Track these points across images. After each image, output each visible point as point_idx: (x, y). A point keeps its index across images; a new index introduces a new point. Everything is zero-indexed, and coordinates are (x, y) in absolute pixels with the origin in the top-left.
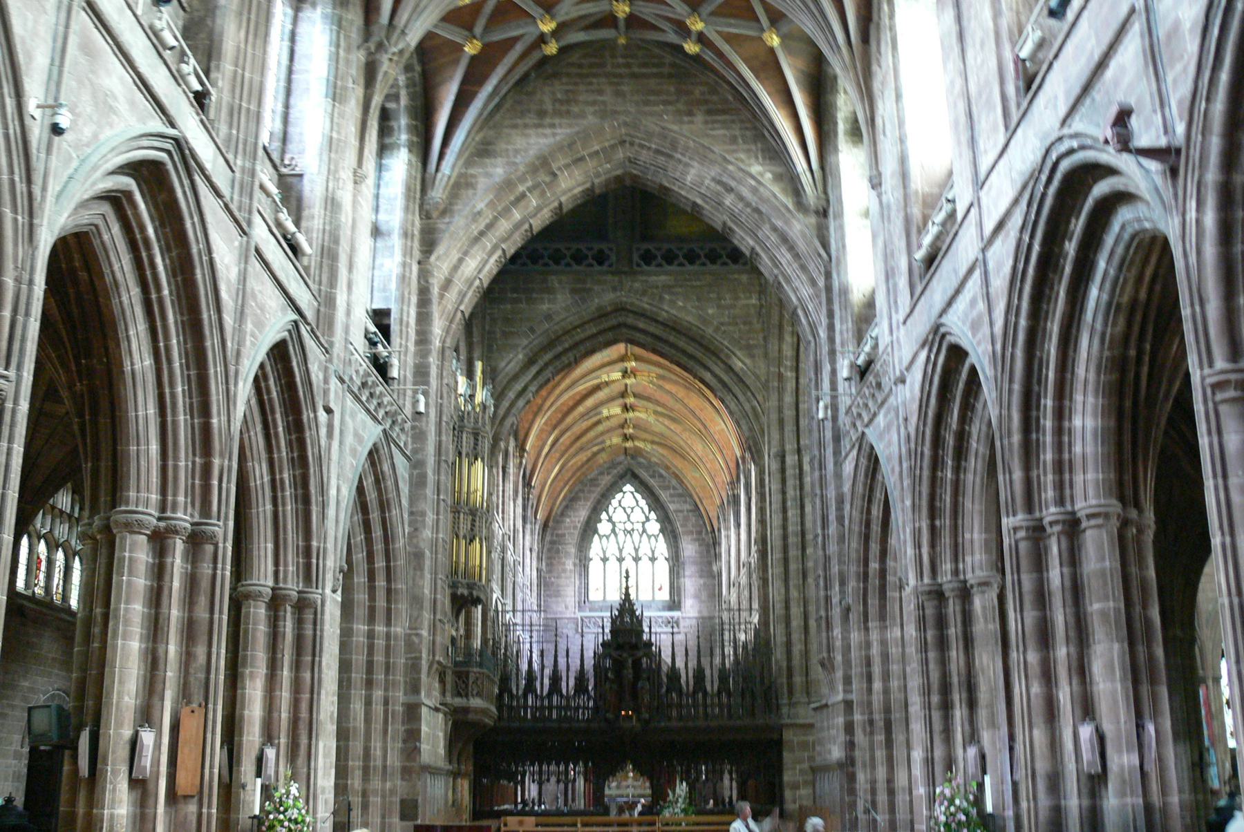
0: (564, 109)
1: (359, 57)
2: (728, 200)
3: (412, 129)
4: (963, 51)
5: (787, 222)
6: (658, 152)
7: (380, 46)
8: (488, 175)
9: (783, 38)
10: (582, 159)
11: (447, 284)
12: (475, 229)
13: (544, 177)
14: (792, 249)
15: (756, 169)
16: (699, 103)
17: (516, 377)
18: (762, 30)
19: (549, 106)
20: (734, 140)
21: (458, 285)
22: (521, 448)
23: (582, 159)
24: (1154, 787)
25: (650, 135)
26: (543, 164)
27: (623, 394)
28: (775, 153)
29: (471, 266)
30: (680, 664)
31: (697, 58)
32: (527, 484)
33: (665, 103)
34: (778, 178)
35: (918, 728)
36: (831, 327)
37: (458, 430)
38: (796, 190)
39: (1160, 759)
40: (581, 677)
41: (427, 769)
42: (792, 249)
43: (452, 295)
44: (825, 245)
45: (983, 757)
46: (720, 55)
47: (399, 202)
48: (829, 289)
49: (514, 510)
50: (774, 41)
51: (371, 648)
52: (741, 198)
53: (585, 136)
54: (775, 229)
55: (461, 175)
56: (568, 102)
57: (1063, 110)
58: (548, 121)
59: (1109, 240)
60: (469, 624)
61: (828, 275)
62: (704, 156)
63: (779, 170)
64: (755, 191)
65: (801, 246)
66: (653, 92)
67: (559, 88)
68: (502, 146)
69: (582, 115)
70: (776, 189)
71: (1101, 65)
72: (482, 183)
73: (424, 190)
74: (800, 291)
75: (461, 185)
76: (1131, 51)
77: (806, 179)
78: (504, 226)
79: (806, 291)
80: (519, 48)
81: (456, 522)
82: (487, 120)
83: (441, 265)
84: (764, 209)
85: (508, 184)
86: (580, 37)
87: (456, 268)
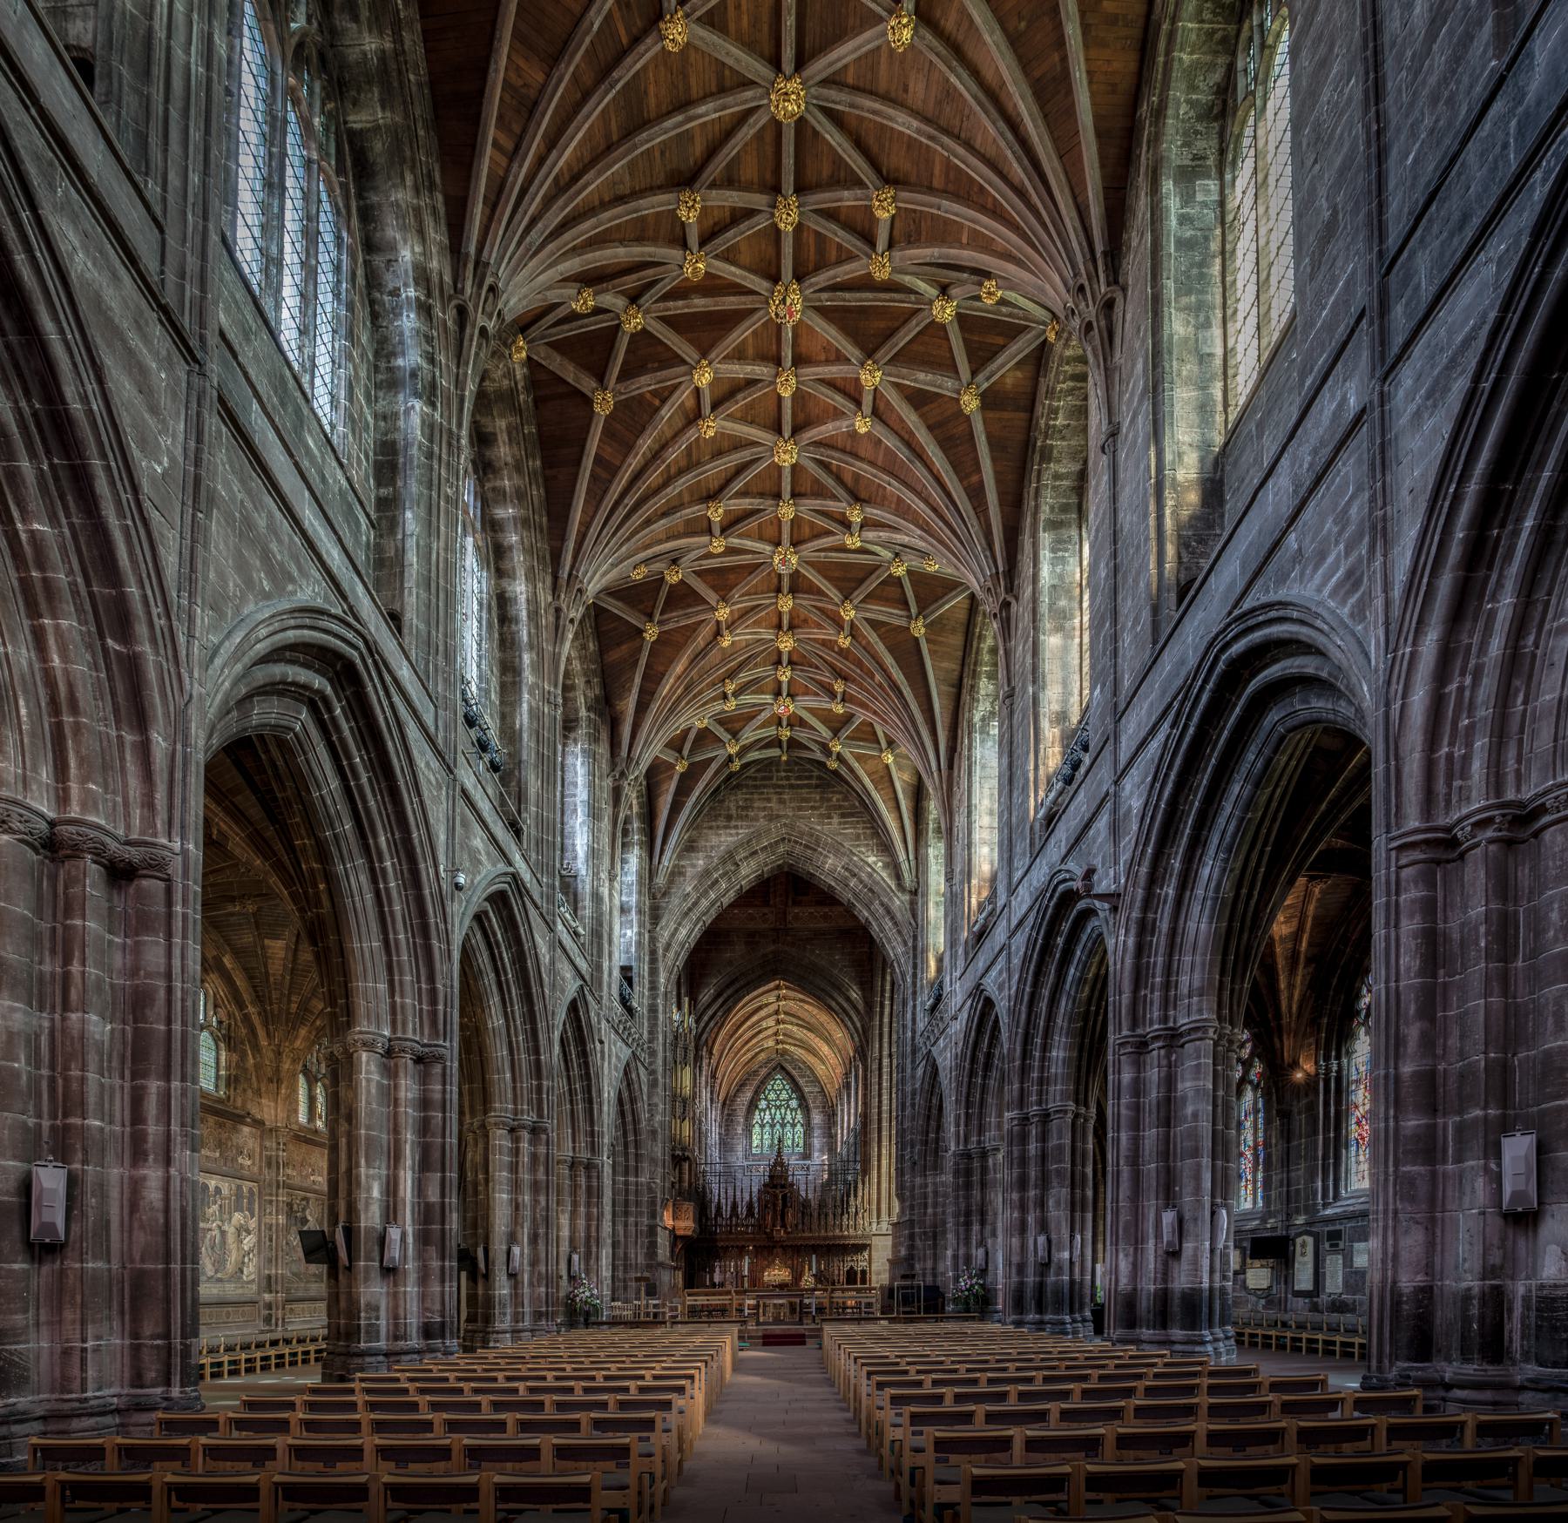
0: (744, 814)
1: (608, 783)
3: (641, 831)
4: (1011, 791)
5: (891, 899)
6: (807, 846)
7: (622, 774)
8: (693, 866)
9: (896, 756)
10: (755, 853)
15: (871, 859)
17: (709, 1006)
18: (881, 751)
19: (734, 812)
20: (858, 837)
22: (711, 1053)
23: (755, 853)
24: (1077, 1270)
25: (802, 834)
26: (730, 856)
27: (777, 1012)
30: (810, 1196)
31: (835, 773)
32: (714, 1076)
34: (886, 866)
35: (950, 1236)
37: (675, 1045)
38: (898, 877)
39: (1082, 1255)
40: (750, 1206)
41: (661, 1265)
42: (892, 918)
44: (914, 916)
45: (987, 1253)
46: (852, 770)
49: (705, 1094)
50: (889, 759)
51: (627, 1191)
52: (861, 882)
53: (758, 835)
54: (882, 904)
55: (675, 866)
56: (745, 808)
57: (1064, 851)
58: (733, 823)
59: (1084, 938)
60: (681, 1173)
61: (915, 938)
62: (837, 850)
63: (888, 860)
64: (870, 876)
65: (899, 915)
69: (756, 819)
70: (884, 875)
71: (1087, 826)
72: (690, 872)
73: (651, 879)
76: (1103, 822)
80: (714, 767)
81: (673, 1108)
82: (693, 824)
84: (876, 889)
85: (707, 873)
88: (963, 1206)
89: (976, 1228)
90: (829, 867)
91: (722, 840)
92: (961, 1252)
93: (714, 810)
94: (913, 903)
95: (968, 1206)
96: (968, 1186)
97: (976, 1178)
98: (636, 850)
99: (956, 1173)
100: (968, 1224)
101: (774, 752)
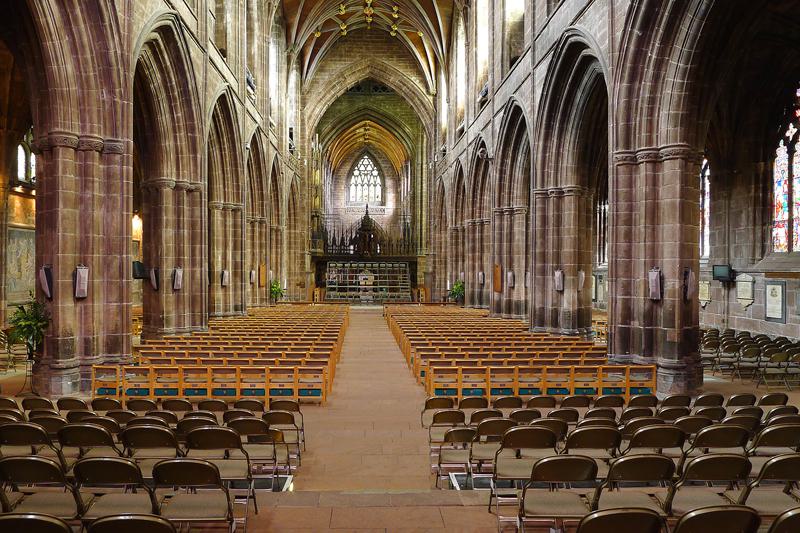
0: (349, 53)
2: (404, 88)
11: (310, 116)
12: (318, 99)
13: (341, 79)
14: (424, 106)
16: (394, 53)
21: (314, 117)
26: (342, 75)
28: (420, 73)
29: (318, 110)
33: (383, 53)
34: (421, 81)
36: (435, 135)
38: (427, 87)
41: (308, 273)
43: (312, 121)
44: (435, 107)
47: (294, 90)
48: (435, 122)
61: (436, 117)
66: (379, 48)
67: (346, 46)
68: (327, 68)
69: (355, 57)
72: (321, 82)
73: (301, 85)
74: (426, 121)
75: (314, 82)
77: (430, 83)
78: (329, 96)
79: (428, 122)
82: (323, 59)
83: (308, 112)
85: (330, 82)
86: (354, 28)
87: (313, 112)
88: (454, 253)
89: (460, 263)
90: (392, 81)
91: (337, 67)
92: (454, 273)
93: (334, 53)
94: (435, 100)
95: (457, 252)
96: (457, 244)
97: (460, 241)
98: (295, 71)
99: (452, 237)
100: (457, 261)
101: (364, 25)
